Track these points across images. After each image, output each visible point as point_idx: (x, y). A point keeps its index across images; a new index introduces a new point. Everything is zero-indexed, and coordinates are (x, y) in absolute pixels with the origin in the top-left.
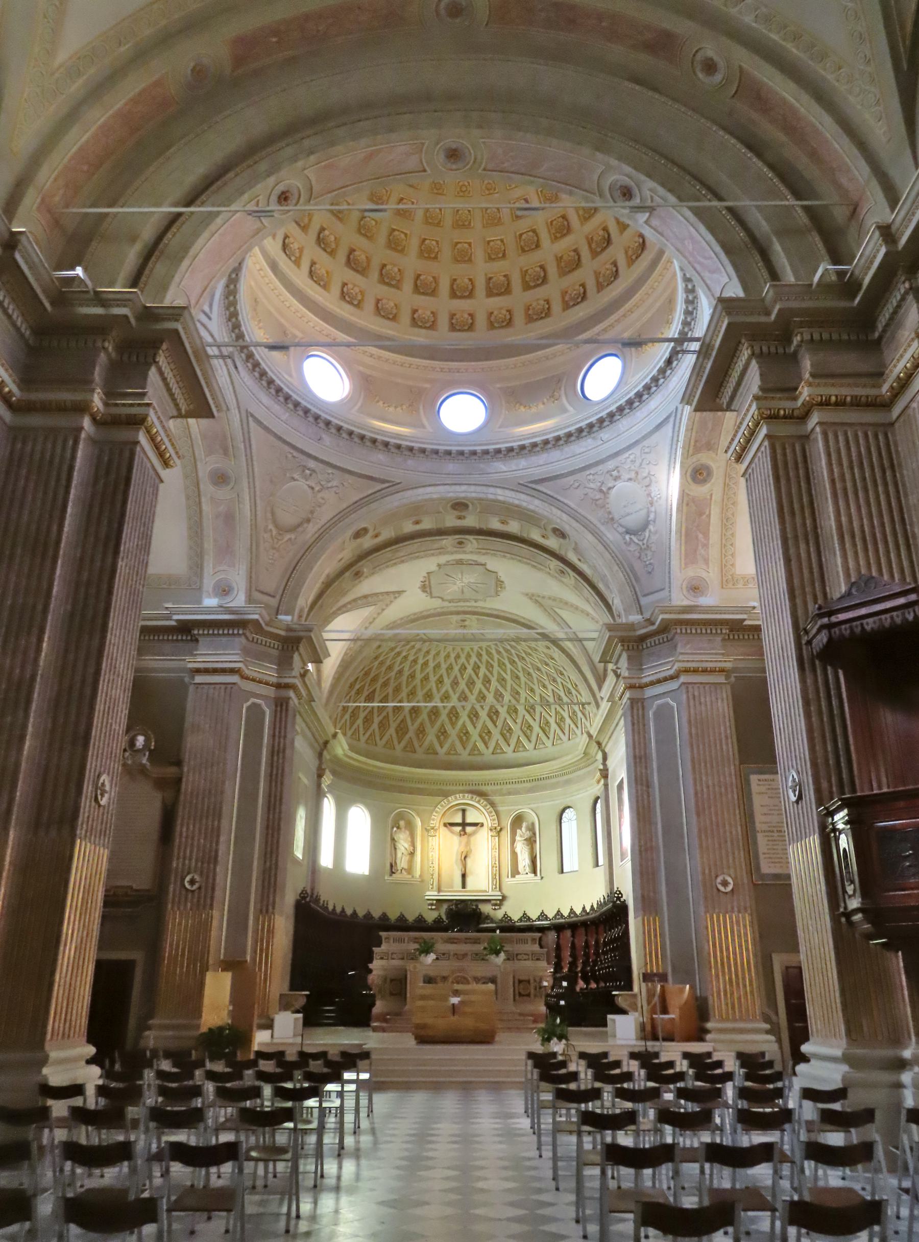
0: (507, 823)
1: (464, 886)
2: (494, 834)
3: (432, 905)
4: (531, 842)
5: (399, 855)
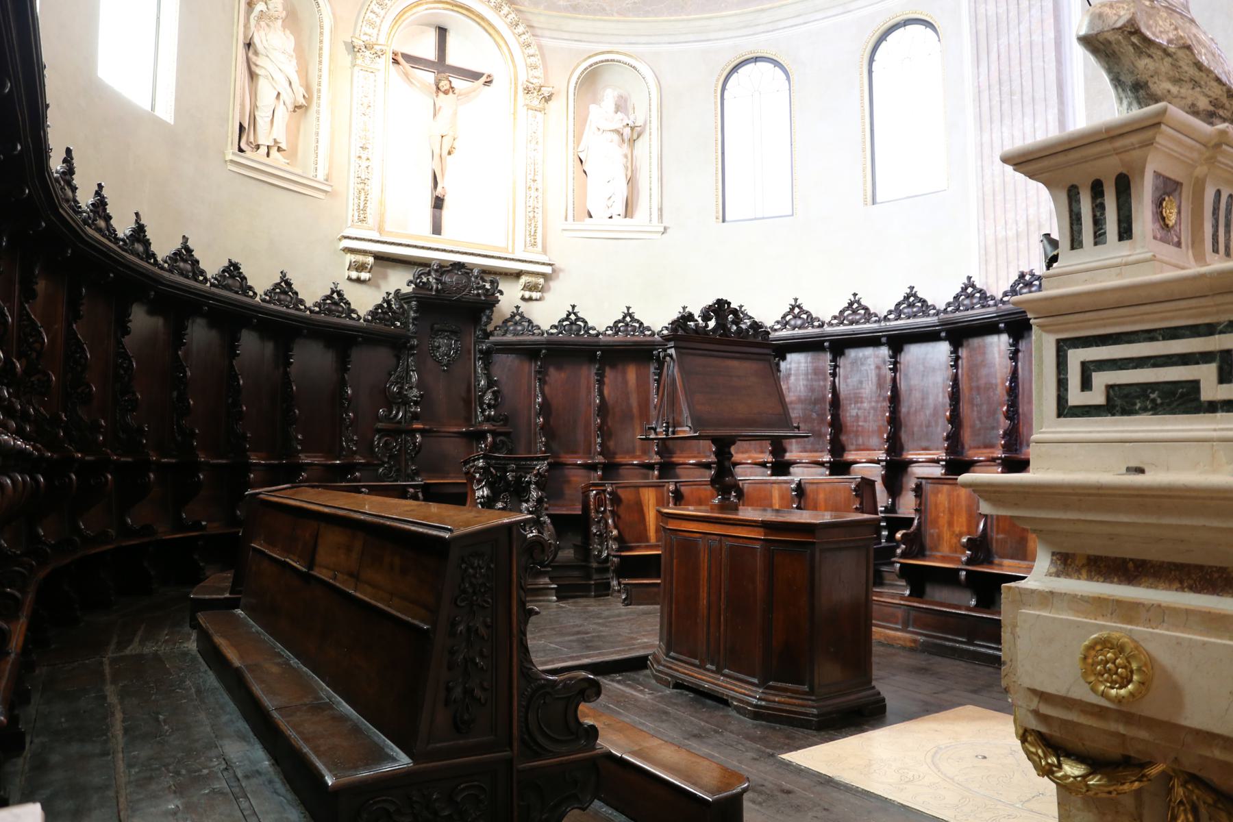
0: (563, 80)
1: (437, 229)
2: (535, 102)
3: (361, 267)
4: (631, 136)
5: (266, 92)
